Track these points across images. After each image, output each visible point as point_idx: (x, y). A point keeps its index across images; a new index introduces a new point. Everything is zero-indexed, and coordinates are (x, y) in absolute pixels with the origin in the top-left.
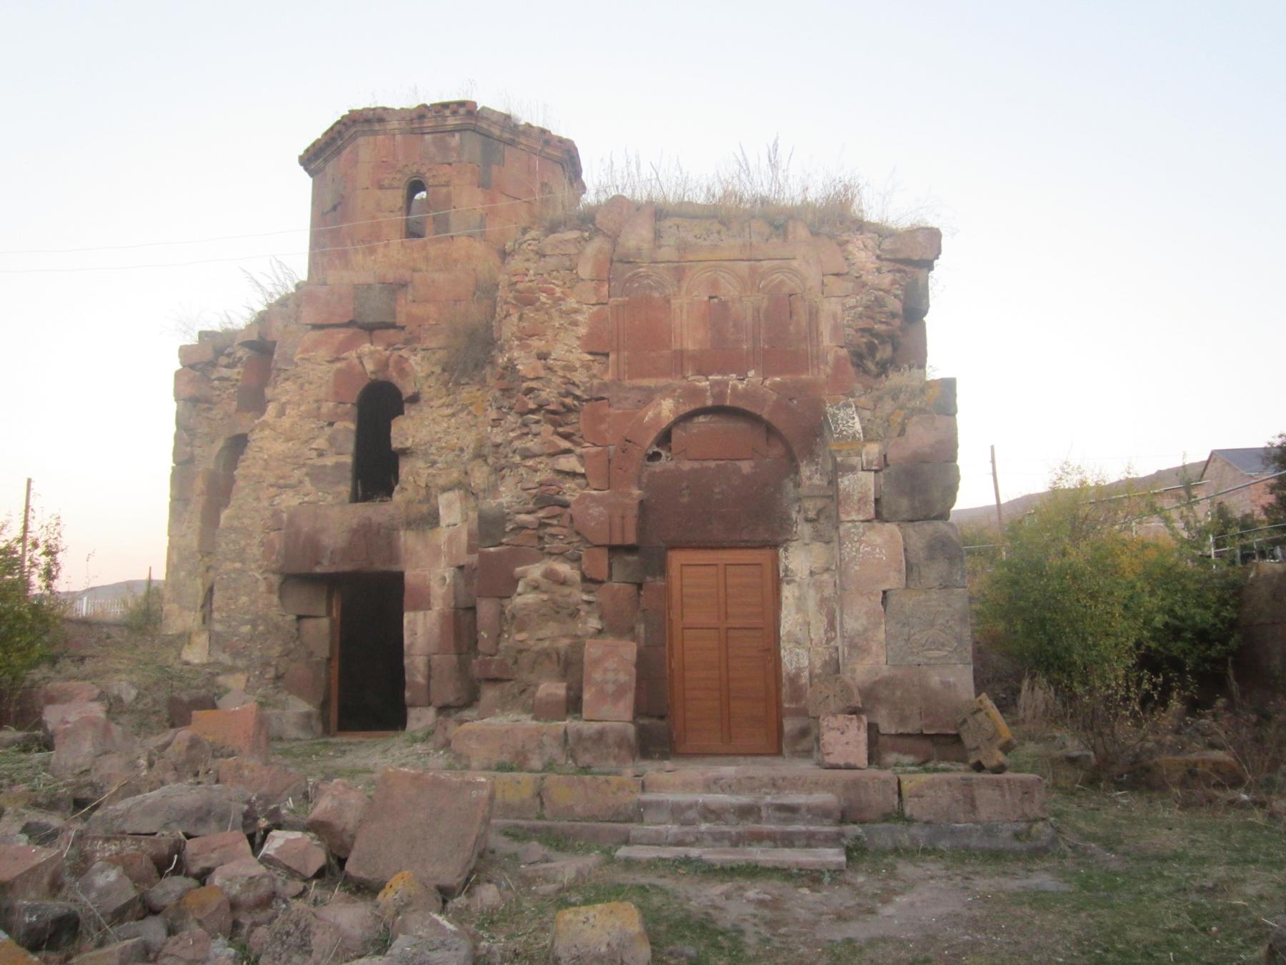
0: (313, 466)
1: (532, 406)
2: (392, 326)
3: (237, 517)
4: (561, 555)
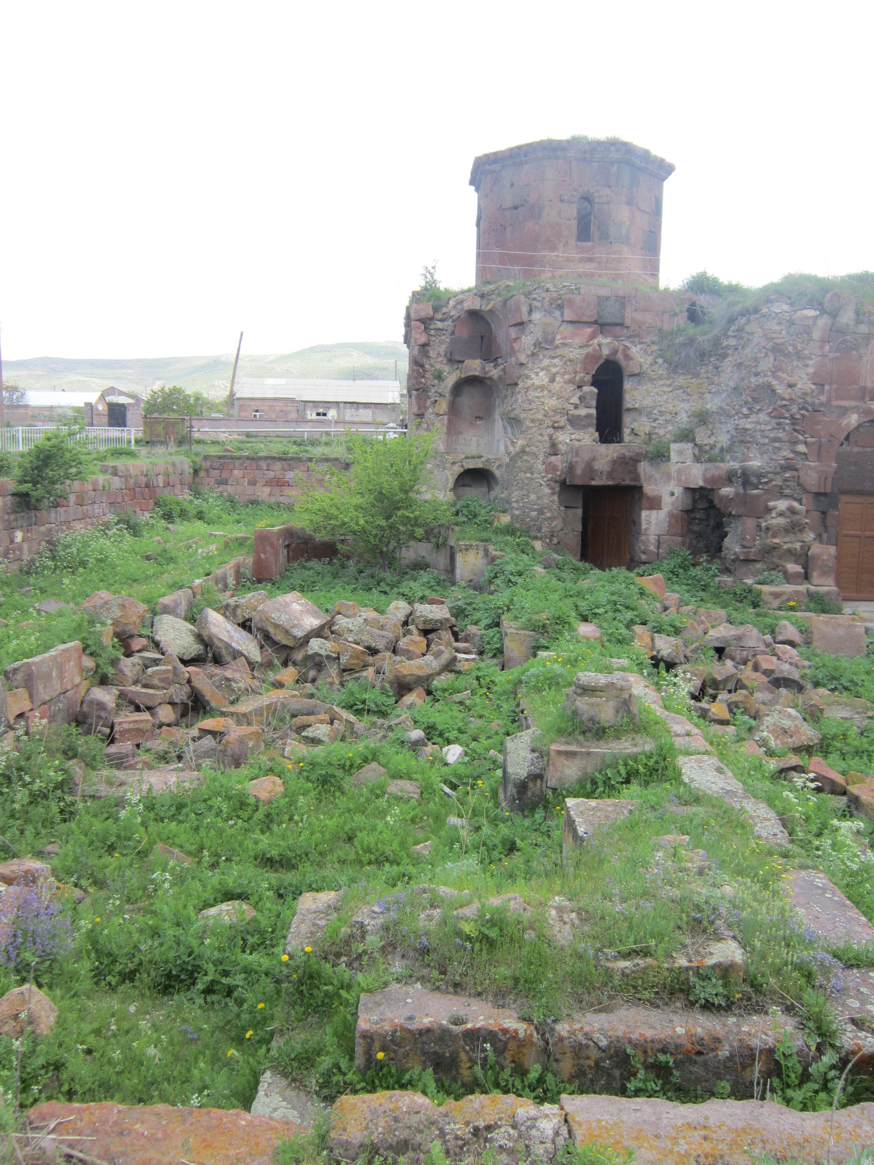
0: (573, 415)
1: (787, 415)
2: (621, 325)
3: (528, 445)
4: (792, 497)
